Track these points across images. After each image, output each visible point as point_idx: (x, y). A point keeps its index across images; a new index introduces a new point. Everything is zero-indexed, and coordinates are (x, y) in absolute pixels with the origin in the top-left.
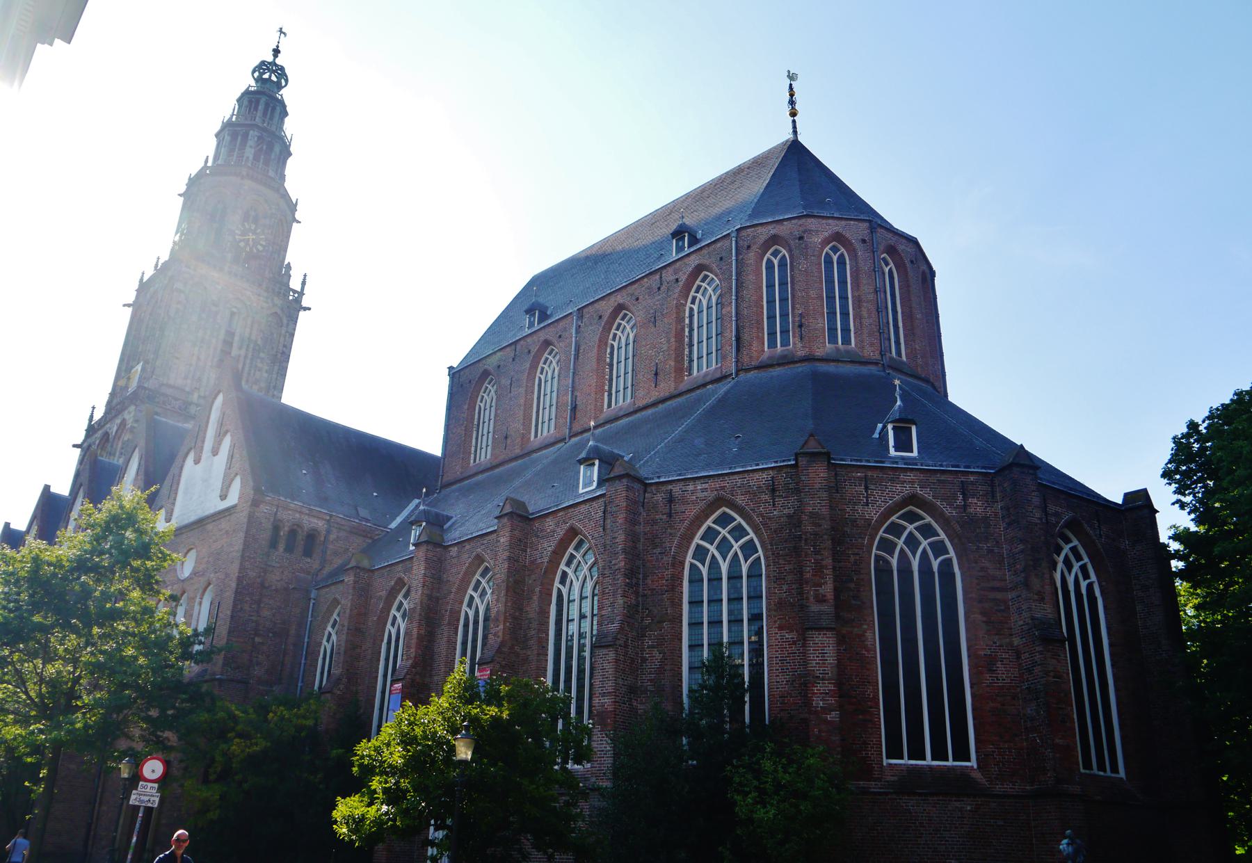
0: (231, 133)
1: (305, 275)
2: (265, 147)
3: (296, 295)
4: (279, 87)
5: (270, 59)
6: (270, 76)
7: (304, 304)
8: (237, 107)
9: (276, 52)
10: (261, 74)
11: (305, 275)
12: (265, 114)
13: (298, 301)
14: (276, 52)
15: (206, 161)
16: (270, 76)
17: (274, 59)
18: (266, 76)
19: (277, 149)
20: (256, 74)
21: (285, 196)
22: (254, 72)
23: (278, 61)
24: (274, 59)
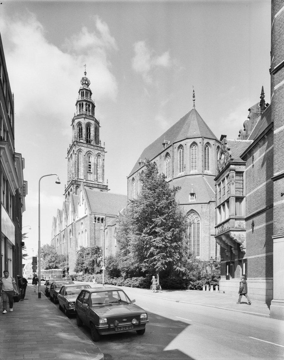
0: (80, 104)
1: (104, 143)
2: (88, 107)
11: (104, 143)
12: (86, 96)
15: (75, 115)
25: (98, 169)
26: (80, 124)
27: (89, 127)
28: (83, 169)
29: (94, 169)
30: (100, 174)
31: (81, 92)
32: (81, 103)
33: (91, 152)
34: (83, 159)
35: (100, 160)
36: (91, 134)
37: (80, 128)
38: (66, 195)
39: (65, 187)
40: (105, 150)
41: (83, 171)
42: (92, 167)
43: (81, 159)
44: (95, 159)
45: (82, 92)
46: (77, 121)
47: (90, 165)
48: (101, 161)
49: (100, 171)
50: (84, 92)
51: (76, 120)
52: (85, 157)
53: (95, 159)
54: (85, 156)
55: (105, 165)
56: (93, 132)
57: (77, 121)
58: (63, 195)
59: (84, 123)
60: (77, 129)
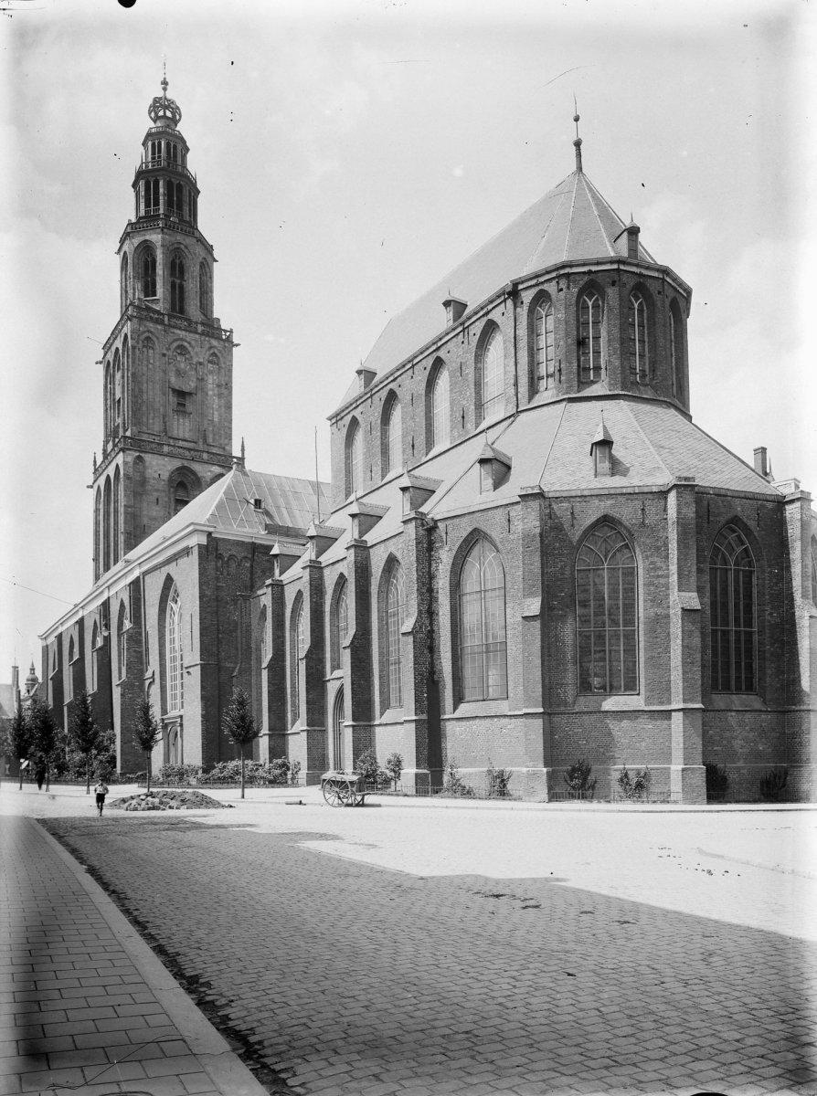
3: (228, 334)
4: (176, 122)
5: (160, 94)
6: (165, 113)
7: (235, 341)
8: (144, 151)
9: (165, 83)
10: (156, 114)
13: (229, 340)
14: (165, 83)
16: (165, 113)
17: (165, 94)
18: (161, 113)
19: (185, 192)
20: (153, 114)
21: (201, 240)
22: (150, 114)
23: (170, 95)
24: (165, 94)
26: (146, 248)
27: (178, 261)
31: (150, 144)
38: (99, 487)
39: (95, 462)
45: (153, 145)
50: (160, 144)
58: (88, 487)
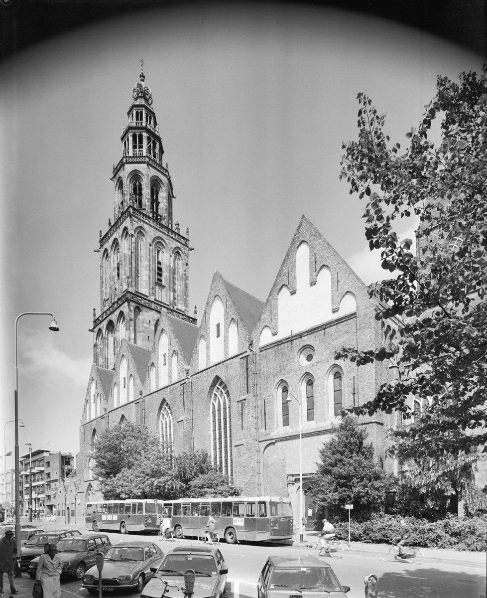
25: (176, 282)
26: (136, 176)
28: (148, 274)
29: (168, 278)
30: (179, 293)
32: (138, 134)
33: (164, 241)
34: (148, 250)
35: (180, 262)
36: (160, 204)
37: (135, 185)
40: (190, 244)
41: (148, 277)
42: (165, 274)
43: (144, 251)
44: (172, 258)
46: (129, 168)
47: (160, 269)
48: (180, 266)
49: (179, 287)
51: (126, 166)
52: (151, 248)
53: (172, 258)
54: (150, 245)
55: (189, 274)
56: (165, 201)
57: (129, 168)
59: (148, 175)
60: (128, 187)
